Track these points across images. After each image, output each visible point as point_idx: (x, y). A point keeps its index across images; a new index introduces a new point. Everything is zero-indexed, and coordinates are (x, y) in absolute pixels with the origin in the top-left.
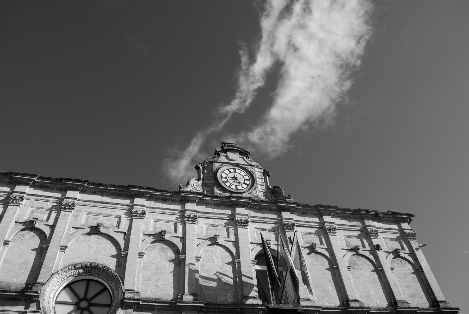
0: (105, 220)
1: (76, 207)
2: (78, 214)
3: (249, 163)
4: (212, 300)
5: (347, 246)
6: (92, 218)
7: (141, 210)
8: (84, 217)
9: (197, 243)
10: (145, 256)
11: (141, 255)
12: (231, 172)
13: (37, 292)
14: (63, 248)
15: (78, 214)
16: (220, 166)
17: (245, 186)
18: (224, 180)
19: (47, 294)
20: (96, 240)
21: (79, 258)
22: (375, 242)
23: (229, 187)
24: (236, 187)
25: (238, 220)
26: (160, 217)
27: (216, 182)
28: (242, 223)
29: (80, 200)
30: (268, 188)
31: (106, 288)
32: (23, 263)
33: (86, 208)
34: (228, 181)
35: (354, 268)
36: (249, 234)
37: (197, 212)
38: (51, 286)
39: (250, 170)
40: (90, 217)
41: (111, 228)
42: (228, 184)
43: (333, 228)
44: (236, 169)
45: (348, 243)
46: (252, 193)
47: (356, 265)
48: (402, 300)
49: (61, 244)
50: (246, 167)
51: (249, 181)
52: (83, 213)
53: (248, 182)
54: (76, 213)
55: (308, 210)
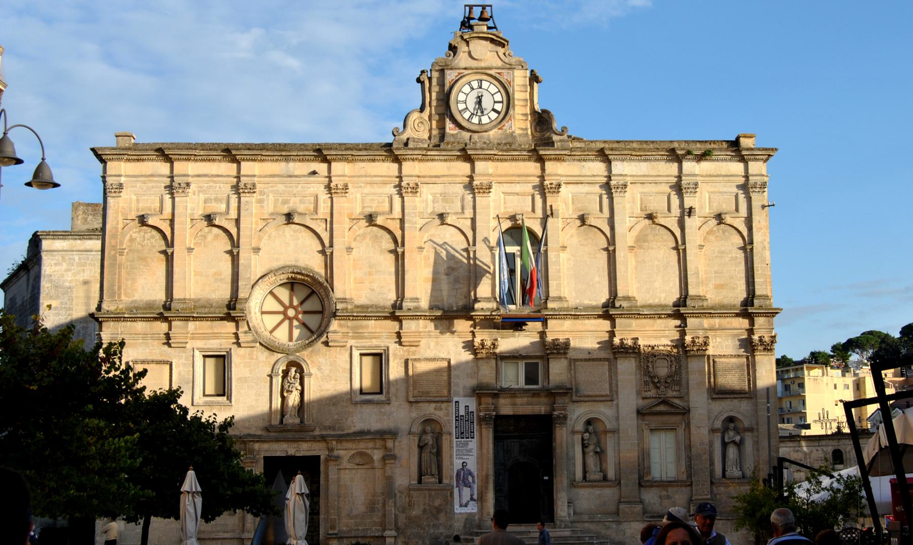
0: (298, 202)
1: (258, 186)
2: (262, 197)
3: (506, 60)
4: (438, 304)
5: (641, 210)
6: (280, 200)
7: (342, 183)
8: (270, 201)
9: (419, 226)
10: (354, 250)
11: (349, 249)
12: (473, 89)
13: (243, 313)
14: (257, 250)
15: (262, 197)
16: (456, 77)
17: (494, 115)
18: (461, 106)
19: (253, 310)
20: (292, 233)
21: (277, 261)
22: (688, 203)
23: (468, 120)
24: (480, 120)
25: (477, 185)
26: (367, 190)
27: (449, 114)
28: (482, 188)
29: (260, 176)
30: (534, 112)
31: (313, 292)
32: (215, 274)
33: (271, 187)
34: (467, 108)
35: (641, 247)
36: (492, 204)
37: (419, 177)
38: (254, 300)
39: (506, 78)
40: (278, 199)
41: (307, 216)
42: (467, 115)
43: (622, 185)
44: (481, 81)
45: (643, 205)
46: (504, 128)
47: (647, 241)
48: (697, 294)
49: (253, 246)
50: (499, 73)
51: (501, 104)
52: (268, 196)
53: (498, 107)
54: (259, 197)
55: (589, 155)
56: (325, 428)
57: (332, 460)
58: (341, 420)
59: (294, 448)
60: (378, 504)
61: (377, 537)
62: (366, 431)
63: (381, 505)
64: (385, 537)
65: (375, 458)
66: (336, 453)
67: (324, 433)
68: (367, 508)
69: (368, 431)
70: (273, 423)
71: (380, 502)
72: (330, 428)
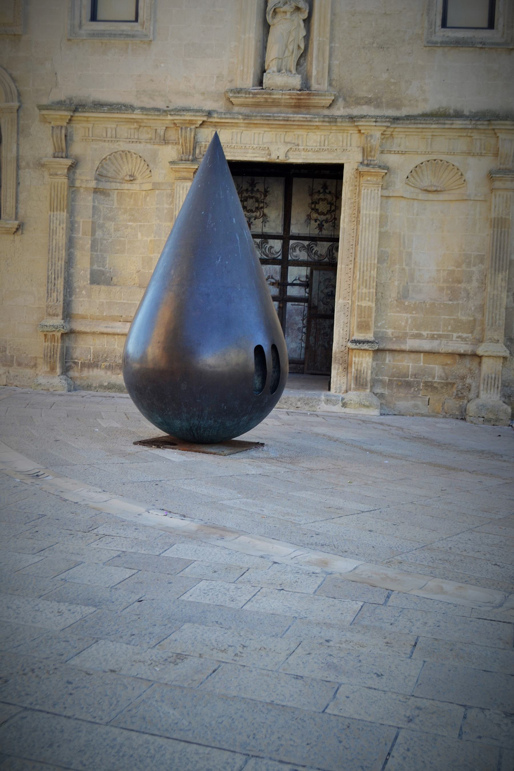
56: (358, 102)
57: (369, 174)
58: (395, 83)
59: (286, 143)
60: (469, 281)
61: (462, 355)
62: (451, 111)
63: (475, 284)
64: (480, 357)
65: (469, 175)
66: (378, 158)
67: (355, 111)
68: (441, 289)
69: (456, 111)
70: (239, 84)
71: (474, 278)
72: (369, 102)
